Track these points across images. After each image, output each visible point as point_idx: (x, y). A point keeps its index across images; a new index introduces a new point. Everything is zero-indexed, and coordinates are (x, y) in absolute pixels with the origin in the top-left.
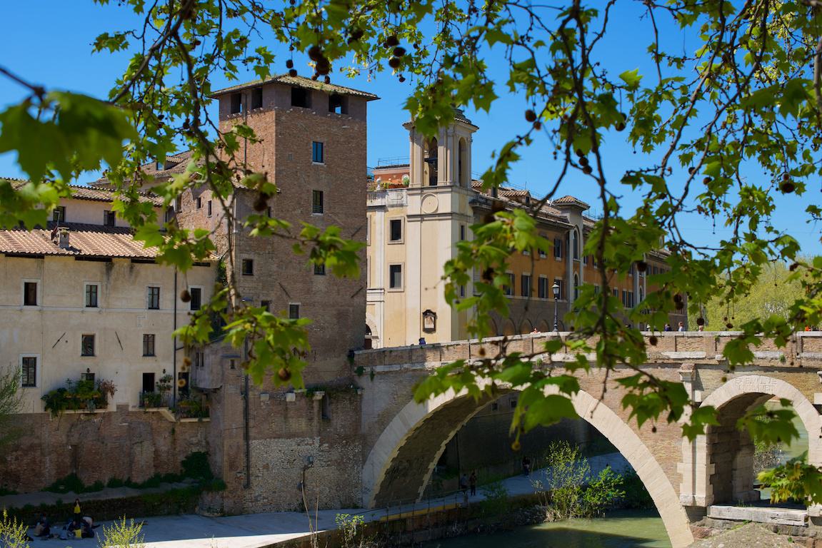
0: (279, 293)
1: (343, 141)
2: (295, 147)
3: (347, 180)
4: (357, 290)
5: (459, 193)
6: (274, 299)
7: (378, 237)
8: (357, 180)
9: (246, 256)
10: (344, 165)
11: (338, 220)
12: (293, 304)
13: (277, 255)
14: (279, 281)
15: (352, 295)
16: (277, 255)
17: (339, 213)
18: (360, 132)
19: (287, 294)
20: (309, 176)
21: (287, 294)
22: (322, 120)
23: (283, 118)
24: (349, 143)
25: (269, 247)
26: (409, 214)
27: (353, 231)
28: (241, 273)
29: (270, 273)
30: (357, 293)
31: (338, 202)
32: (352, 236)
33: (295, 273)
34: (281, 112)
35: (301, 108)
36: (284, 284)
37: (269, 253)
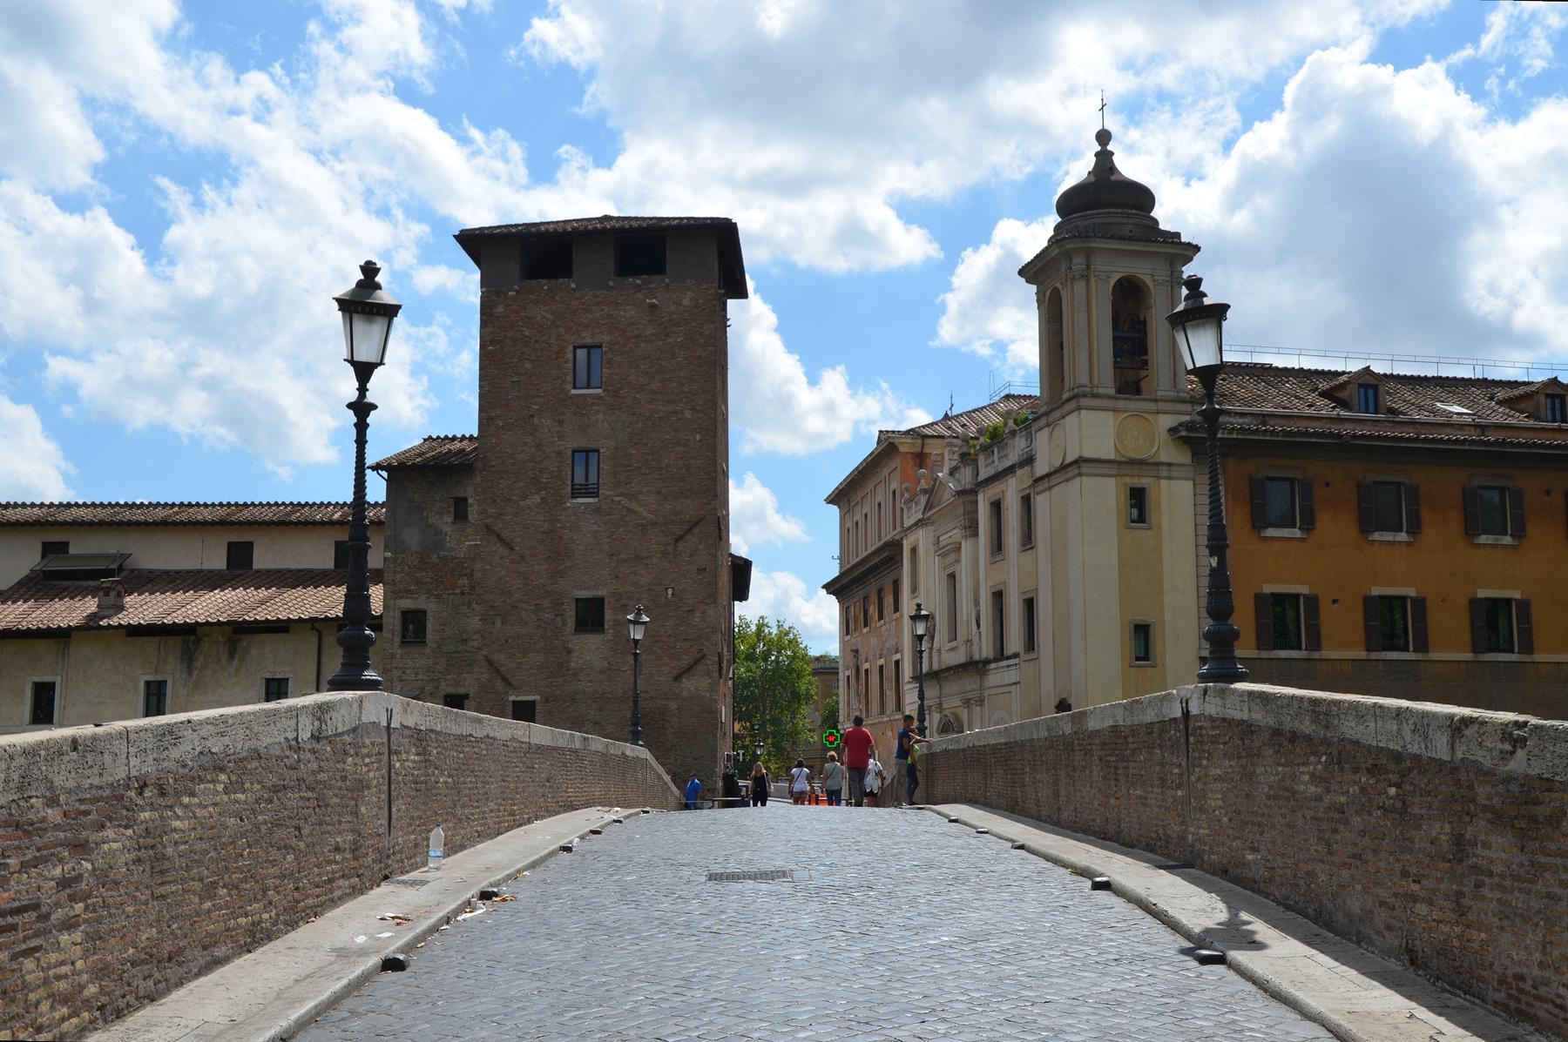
1: (651, 334)
3: (661, 418)
5: (1115, 410)
6: (472, 691)
7: (1011, 537)
8: (688, 414)
9: (407, 604)
11: (641, 510)
12: (519, 699)
15: (675, 672)
19: (504, 679)
20: (561, 422)
21: (504, 679)
23: (501, 309)
24: (668, 335)
25: (464, 581)
28: (398, 639)
29: (465, 636)
30: (690, 668)
31: (638, 468)
32: (677, 541)
34: (494, 297)
35: (545, 281)
37: (462, 594)
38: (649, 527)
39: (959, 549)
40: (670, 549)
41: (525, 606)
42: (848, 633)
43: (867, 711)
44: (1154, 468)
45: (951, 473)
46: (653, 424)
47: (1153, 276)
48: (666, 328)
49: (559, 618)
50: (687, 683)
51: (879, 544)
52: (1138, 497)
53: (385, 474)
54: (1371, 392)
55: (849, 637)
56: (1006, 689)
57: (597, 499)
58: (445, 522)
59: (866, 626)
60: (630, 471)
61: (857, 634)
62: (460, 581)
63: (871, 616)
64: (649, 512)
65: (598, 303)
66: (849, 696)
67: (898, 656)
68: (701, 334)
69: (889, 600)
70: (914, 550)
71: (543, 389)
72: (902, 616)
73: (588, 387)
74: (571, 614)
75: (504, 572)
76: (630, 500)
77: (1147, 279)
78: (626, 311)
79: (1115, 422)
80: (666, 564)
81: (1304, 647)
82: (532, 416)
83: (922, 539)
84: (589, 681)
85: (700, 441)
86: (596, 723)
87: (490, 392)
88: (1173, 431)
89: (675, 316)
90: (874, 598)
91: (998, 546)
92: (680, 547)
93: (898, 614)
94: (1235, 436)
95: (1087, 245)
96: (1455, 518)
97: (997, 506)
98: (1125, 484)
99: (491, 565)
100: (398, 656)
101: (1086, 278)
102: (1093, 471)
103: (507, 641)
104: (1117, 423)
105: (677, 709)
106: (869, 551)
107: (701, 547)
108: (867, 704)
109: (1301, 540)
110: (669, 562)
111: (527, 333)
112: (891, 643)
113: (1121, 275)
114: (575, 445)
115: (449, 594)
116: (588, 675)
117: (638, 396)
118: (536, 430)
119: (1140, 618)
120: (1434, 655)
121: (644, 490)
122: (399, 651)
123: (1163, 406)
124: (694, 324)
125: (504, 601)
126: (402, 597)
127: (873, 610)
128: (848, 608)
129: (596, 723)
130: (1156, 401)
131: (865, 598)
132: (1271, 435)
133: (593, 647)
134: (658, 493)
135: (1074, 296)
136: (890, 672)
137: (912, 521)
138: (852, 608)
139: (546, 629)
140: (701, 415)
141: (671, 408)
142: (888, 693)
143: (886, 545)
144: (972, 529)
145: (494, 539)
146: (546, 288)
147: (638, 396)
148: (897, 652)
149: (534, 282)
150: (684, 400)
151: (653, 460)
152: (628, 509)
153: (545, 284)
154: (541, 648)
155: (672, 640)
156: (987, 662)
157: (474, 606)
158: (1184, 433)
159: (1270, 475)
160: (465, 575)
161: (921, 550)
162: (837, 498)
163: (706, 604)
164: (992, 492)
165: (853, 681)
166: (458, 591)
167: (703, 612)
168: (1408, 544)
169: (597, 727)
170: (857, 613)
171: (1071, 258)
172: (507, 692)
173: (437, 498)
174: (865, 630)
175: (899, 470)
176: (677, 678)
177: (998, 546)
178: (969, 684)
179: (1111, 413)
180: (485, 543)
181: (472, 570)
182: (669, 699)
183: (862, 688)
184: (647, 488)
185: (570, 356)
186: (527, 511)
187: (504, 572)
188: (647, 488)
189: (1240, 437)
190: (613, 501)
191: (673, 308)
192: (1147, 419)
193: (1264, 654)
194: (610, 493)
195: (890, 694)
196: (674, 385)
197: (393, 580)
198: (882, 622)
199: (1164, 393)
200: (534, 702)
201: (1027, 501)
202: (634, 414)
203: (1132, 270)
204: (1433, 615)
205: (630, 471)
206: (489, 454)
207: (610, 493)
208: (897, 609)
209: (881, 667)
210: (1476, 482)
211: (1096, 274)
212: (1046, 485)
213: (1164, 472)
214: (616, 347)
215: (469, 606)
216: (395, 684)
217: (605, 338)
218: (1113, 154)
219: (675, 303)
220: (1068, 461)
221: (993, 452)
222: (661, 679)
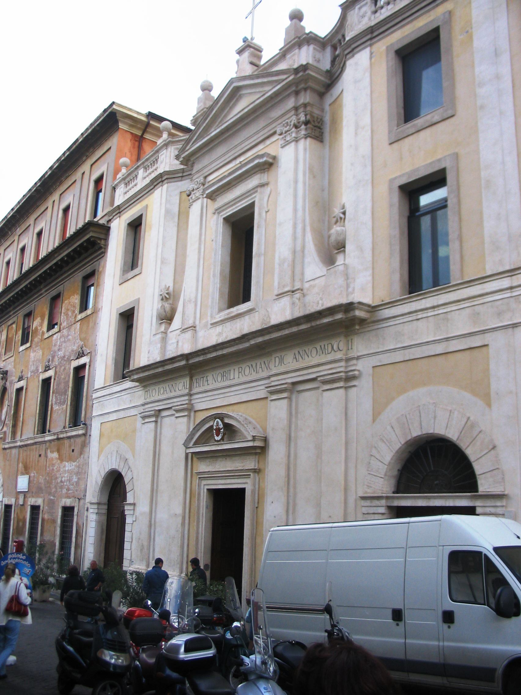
43: (14, 433)
59: (25, 340)
67: (84, 360)
72: (96, 311)
108: (15, 426)
142: (56, 407)
148: (81, 355)
156: (373, 309)
174: (22, 348)
209: (46, 382)
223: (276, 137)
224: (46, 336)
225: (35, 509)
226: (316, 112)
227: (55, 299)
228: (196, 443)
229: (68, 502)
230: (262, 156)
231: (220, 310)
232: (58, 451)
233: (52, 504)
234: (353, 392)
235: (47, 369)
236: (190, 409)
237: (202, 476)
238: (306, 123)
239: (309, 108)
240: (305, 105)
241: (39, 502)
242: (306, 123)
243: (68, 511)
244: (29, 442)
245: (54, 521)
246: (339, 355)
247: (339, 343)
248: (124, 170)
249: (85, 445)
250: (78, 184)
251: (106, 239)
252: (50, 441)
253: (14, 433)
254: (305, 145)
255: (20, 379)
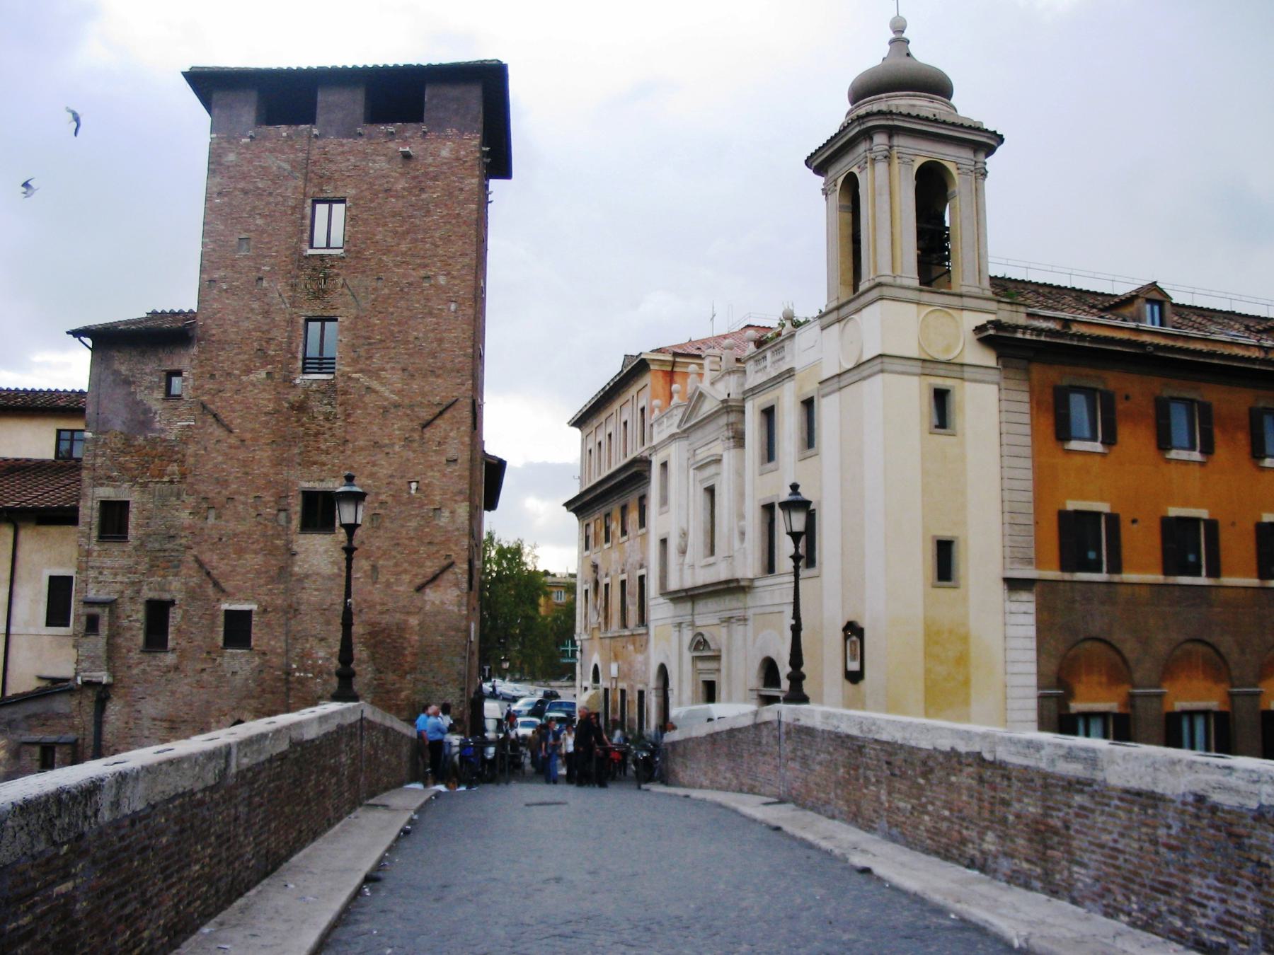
0: (194, 581)
1: (404, 189)
2: (260, 221)
3: (410, 284)
4: (436, 569)
5: (918, 303)
6: (179, 597)
8: (442, 280)
10: (404, 247)
11: (383, 389)
13: (192, 484)
14: (194, 552)
15: (419, 581)
16: (192, 484)
17: (383, 369)
18: (458, 159)
19: (216, 584)
21: (216, 584)
22: (342, 145)
23: (231, 157)
24: (422, 190)
25: (174, 468)
26: (825, 376)
27: (425, 414)
28: (95, 533)
29: (172, 532)
30: (435, 578)
31: (381, 341)
33: (240, 528)
36: (206, 557)
37: (171, 482)
38: (393, 410)
39: (718, 461)
40: (416, 436)
41: (242, 498)
42: (587, 548)
43: (606, 623)
44: (958, 368)
45: (712, 384)
46: (401, 290)
47: (957, 164)
48: (420, 182)
49: (282, 515)
50: (431, 595)
51: (623, 462)
52: (941, 397)
53: (89, 341)
54: (1156, 308)
55: (588, 553)
56: (780, 608)
57: (331, 377)
58: (154, 400)
59: (607, 540)
60: (370, 344)
61: (598, 548)
62: (169, 468)
63: (613, 533)
64: (392, 392)
65: (343, 153)
66: (586, 608)
67: (643, 572)
68: (461, 190)
69: (633, 516)
70: (664, 465)
71: (275, 249)
72: (647, 532)
73: (328, 247)
74: (296, 507)
75: (220, 459)
76: (370, 377)
77: (951, 167)
78: (374, 162)
79: (918, 316)
80: (410, 453)
81: (1105, 568)
82: (261, 279)
83: (676, 454)
84: (316, 590)
85: (455, 312)
86: (322, 640)
87: (214, 250)
88: (979, 329)
89: (431, 169)
90: (616, 513)
91: (770, 453)
92: (428, 433)
93: (643, 530)
94: (1043, 338)
95: (890, 123)
96: (1243, 439)
97: (769, 414)
98: (930, 384)
99: (205, 449)
100: (95, 554)
101: (888, 158)
102: (899, 368)
103: (220, 539)
104: (921, 318)
105: (419, 625)
106: (614, 468)
107: (451, 434)
108: (606, 617)
109: (1103, 455)
110: (414, 451)
111: (260, 185)
112: (635, 558)
113: (923, 160)
114: (310, 314)
115: (157, 483)
116: (315, 582)
117: (385, 258)
118: (265, 295)
119: (945, 534)
120: (1226, 580)
121: (388, 366)
122: (96, 548)
123: (967, 302)
124: (454, 178)
125: (219, 493)
126: (102, 485)
127: (615, 527)
128: (588, 525)
129: (322, 640)
130: (961, 296)
131: (608, 515)
132: (1078, 341)
133: (322, 549)
134: (404, 370)
135: (872, 181)
136: (633, 587)
137: (665, 435)
138: (592, 526)
139: (266, 526)
140: (457, 282)
141: (422, 272)
142: (630, 607)
143: (634, 462)
144: (739, 439)
145: (210, 419)
146: (284, 134)
147: (385, 258)
148: (641, 566)
149: (271, 128)
150: (439, 264)
151: (400, 332)
152: (368, 388)
153: (284, 130)
154: (261, 549)
155: (414, 543)
156: (752, 580)
157: (184, 497)
158: (992, 332)
159: (1074, 383)
160: (175, 461)
161: (672, 467)
162: (580, 421)
163: (456, 502)
164: (763, 400)
165: (591, 595)
166: (166, 479)
167: (452, 512)
168: (1202, 464)
169: (323, 644)
170: (598, 527)
171: (871, 139)
172: (218, 600)
173: (147, 371)
174: (606, 546)
175: (648, 389)
176: (420, 589)
177: (770, 453)
178: (728, 605)
179: (914, 306)
180: (199, 424)
181: (184, 456)
182: (408, 613)
183: (601, 602)
184: (392, 365)
185: (308, 211)
186: (250, 388)
187: (220, 459)
188: (392, 365)
189: (1048, 340)
190: (350, 378)
191: (430, 160)
192: (950, 314)
193: (1067, 576)
194: (348, 369)
195: (633, 610)
196: (428, 246)
197: (93, 465)
198: (625, 538)
199: (969, 289)
200: (249, 612)
201: (808, 404)
202: (379, 279)
203: (935, 155)
204: (1225, 537)
205: (370, 344)
206: (209, 321)
207: (348, 369)
208: (642, 523)
209: (623, 583)
210: (1261, 404)
211: (900, 155)
212: (836, 386)
213: (968, 373)
214: (361, 202)
215: (178, 496)
216: (90, 586)
217: (351, 192)
218: (908, 42)
219: (431, 154)
220: (866, 357)
221: (765, 358)
222: (399, 588)
223: (719, 441)
224: (621, 541)
225: (623, 692)
226: (740, 426)
227: (624, 509)
228: (696, 649)
229: (640, 687)
230: (712, 456)
231: (705, 557)
232: (634, 644)
233: (632, 687)
234: (748, 627)
235: (623, 572)
236: (692, 624)
237: (700, 672)
238: (733, 437)
239: (735, 426)
240: (732, 424)
241: (623, 685)
242: (733, 437)
243: (641, 693)
244: (616, 634)
245: (634, 701)
246: (740, 605)
247: (741, 596)
248: (657, 412)
249: (647, 641)
250: (630, 402)
251: (650, 470)
252: (628, 636)
253: (606, 623)
254: (733, 452)
255: (607, 575)
